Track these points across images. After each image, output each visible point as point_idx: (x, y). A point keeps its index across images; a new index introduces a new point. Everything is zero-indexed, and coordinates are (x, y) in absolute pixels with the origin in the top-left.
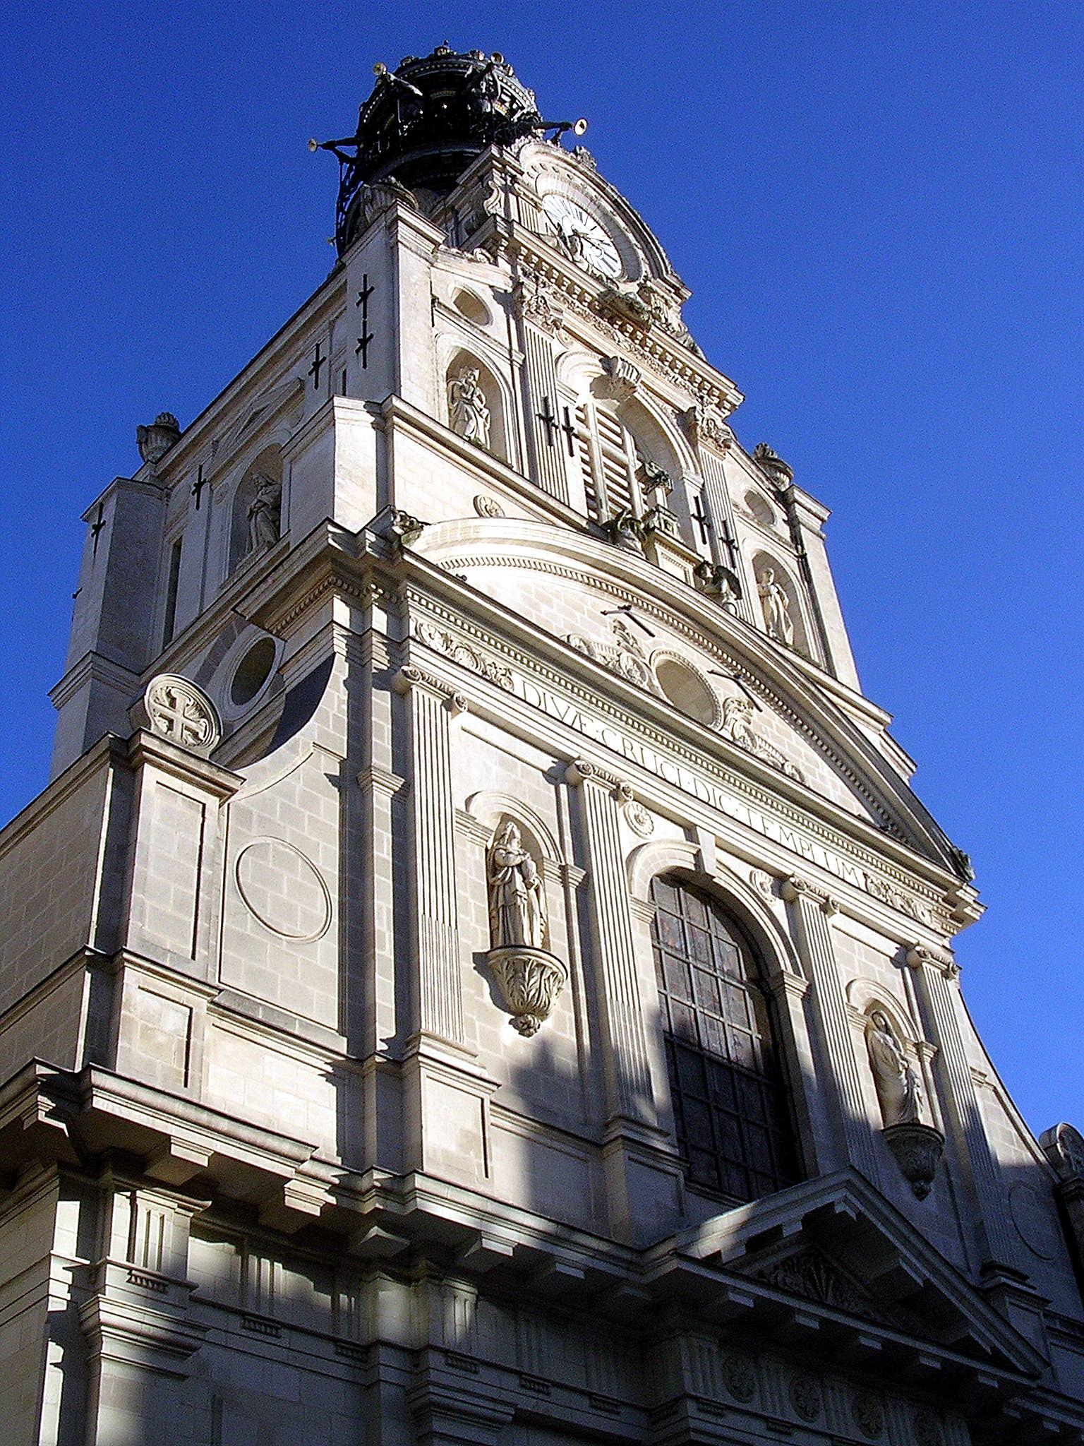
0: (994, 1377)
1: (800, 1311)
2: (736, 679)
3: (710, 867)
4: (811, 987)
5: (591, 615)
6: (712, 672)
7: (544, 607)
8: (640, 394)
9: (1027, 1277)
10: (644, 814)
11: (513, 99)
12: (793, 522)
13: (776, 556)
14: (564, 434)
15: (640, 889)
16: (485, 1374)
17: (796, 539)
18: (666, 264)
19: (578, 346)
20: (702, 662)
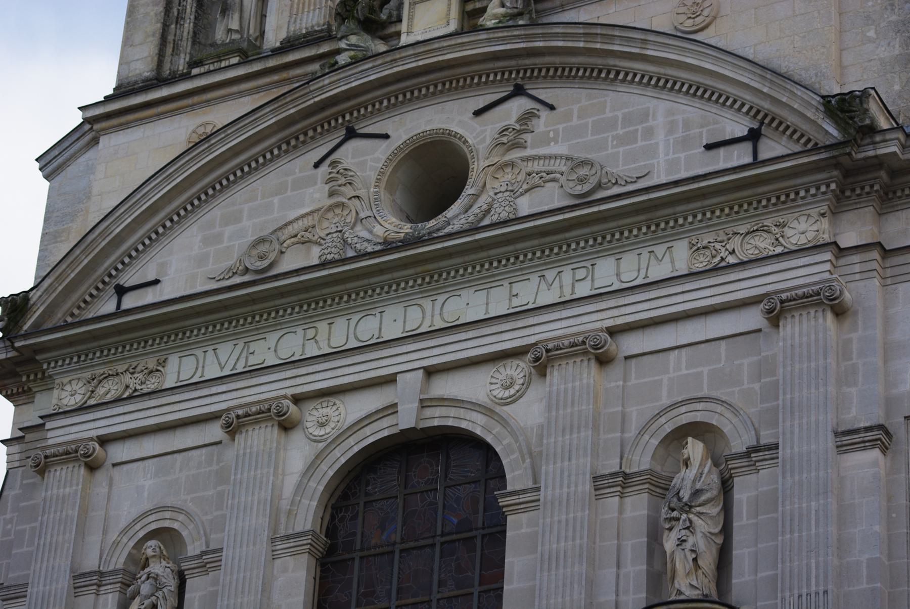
2: (519, 91)
3: (407, 419)
6: (478, 113)
7: (229, 230)
15: (307, 516)
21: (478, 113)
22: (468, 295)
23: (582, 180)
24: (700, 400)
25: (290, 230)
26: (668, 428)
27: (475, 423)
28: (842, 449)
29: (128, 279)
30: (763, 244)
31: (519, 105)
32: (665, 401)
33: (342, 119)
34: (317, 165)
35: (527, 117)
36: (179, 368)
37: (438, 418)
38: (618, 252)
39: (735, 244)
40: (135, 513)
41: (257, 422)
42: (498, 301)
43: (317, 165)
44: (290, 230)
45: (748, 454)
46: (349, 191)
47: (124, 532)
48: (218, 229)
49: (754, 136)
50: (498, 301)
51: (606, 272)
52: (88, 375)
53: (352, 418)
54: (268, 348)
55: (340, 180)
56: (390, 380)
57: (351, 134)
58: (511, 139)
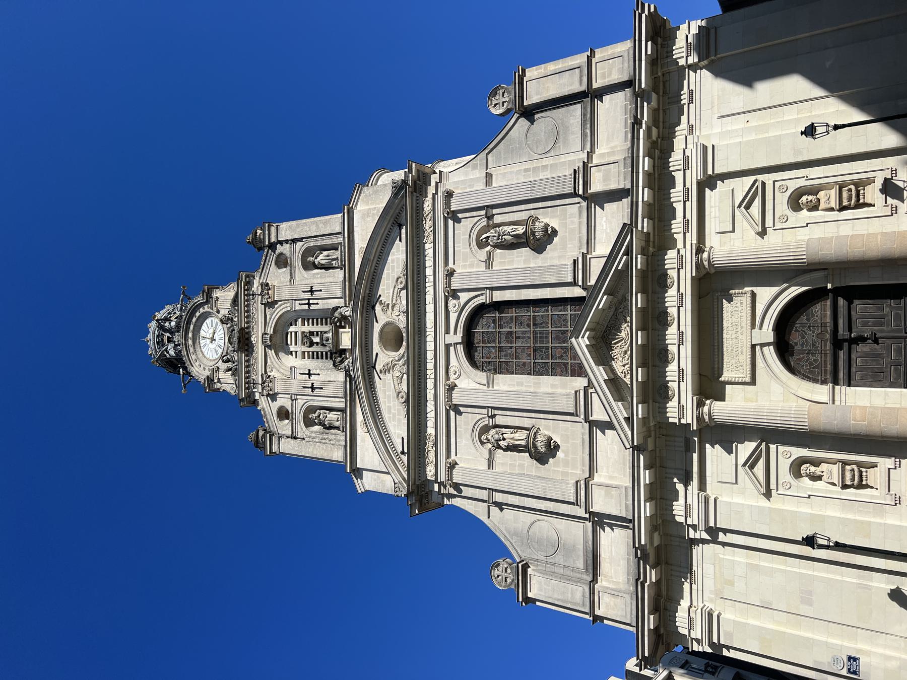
0: (636, 258)
1: (637, 379)
2: (373, 308)
3: (458, 338)
4: (487, 288)
5: (384, 386)
8: (270, 331)
9: (575, 171)
10: (451, 371)
12: (281, 243)
13: (300, 256)
14: (313, 377)
15: (482, 376)
16: (689, 501)
17: (286, 241)
18: (199, 299)
20: (377, 328)
23: (401, 283)
26: (476, 247)
27: (465, 314)
28: (491, 184)
29: (400, 449)
31: (378, 308)
32: (468, 250)
33: (369, 367)
35: (381, 304)
36: (431, 430)
47: (477, 450)
51: (429, 272)
55: (387, 369)
56: (448, 346)
57: (374, 367)
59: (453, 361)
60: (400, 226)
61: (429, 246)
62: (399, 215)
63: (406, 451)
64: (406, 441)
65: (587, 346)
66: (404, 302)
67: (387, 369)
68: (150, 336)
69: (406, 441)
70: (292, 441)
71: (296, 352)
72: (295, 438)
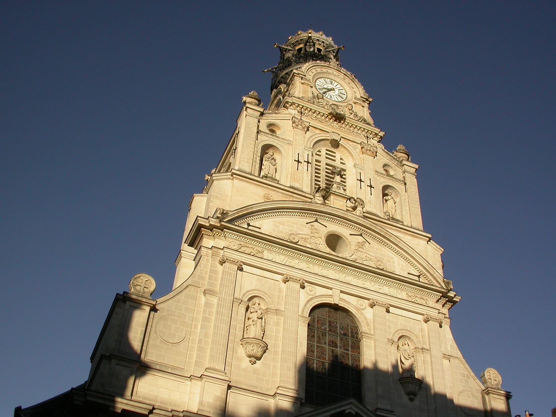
2: (361, 235)
6: (350, 235)
7: (281, 227)
11: (323, 42)
19: (318, 131)
21: (350, 235)
22: (351, 278)
23: (380, 265)
24: (409, 331)
25: (303, 236)
30: (424, 303)
32: (399, 327)
34: (307, 223)
37: (342, 304)
38: (390, 287)
39: (417, 299)
40: (249, 289)
41: (294, 281)
42: (360, 283)
43: (307, 223)
44: (300, 236)
45: (422, 349)
46: (317, 235)
48: (277, 224)
49: (419, 276)
50: (360, 283)
52: (238, 242)
53: (318, 294)
54: (295, 262)
55: (314, 231)
56: (331, 289)
57: (316, 221)
58: (361, 245)
59: (320, 291)
60: (419, 276)
61: (403, 295)
62: (426, 277)
63: (250, 228)
64: (257, 230)
65: (345, 410)
66: (365, 263)
67: (314, 231)
68: (324, 37)
69: (257, 230)
70: (256, 131)
71: (320, 155)
72: (258, 132)
